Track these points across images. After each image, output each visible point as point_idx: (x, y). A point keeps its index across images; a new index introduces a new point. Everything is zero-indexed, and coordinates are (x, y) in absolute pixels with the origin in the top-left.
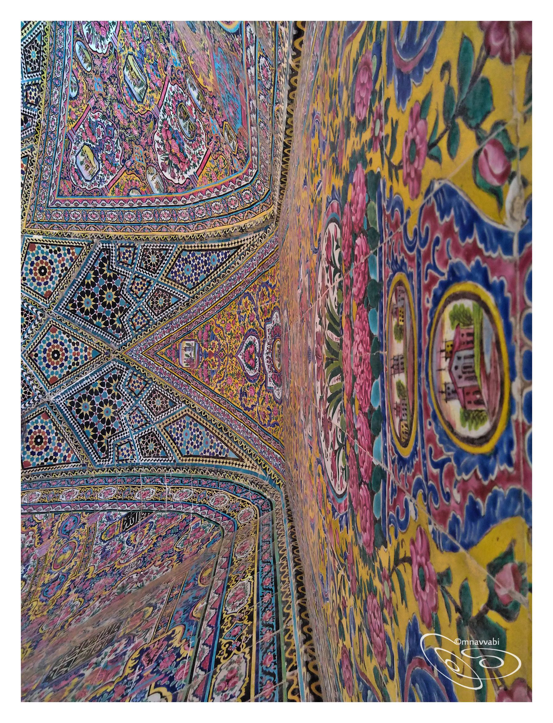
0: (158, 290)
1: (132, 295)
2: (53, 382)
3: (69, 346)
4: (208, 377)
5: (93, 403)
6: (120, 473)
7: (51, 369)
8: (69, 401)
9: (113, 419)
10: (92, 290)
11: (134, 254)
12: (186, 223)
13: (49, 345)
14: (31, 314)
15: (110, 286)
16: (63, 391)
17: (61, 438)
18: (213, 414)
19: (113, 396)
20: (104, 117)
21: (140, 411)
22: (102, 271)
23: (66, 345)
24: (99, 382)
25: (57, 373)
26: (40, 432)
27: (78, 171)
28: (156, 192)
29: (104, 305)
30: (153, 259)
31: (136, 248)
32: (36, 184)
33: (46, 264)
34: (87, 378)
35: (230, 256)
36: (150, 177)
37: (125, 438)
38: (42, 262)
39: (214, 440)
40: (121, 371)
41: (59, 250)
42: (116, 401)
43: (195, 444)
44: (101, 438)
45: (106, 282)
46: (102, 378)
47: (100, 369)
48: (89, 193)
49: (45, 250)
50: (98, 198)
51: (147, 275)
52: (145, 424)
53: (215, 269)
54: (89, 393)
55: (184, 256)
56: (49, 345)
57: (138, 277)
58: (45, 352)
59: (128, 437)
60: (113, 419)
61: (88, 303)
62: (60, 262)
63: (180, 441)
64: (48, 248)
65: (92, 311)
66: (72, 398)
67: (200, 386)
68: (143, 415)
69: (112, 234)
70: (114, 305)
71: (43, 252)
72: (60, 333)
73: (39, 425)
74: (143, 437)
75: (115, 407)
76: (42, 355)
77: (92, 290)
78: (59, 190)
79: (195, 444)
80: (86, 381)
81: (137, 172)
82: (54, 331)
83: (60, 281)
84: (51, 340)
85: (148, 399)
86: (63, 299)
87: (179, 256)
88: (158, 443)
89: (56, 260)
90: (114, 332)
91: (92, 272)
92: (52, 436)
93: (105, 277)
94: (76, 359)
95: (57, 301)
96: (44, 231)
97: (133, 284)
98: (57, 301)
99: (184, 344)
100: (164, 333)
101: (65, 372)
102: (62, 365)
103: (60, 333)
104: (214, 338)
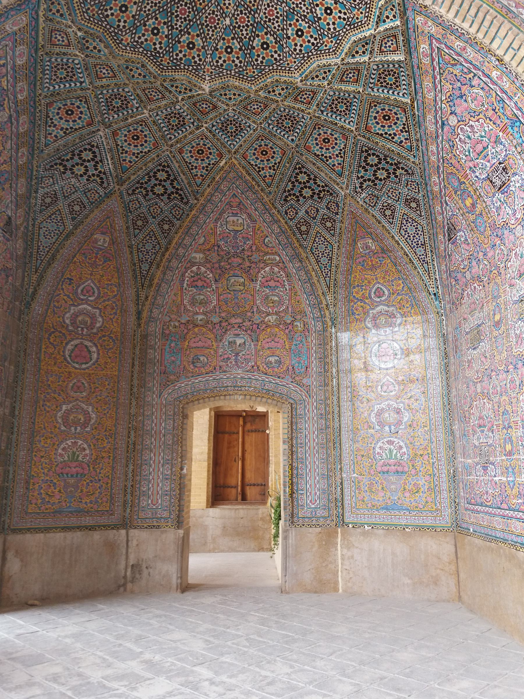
0: (147, 222)
1: (153, 203)
2: (115, 134)
3: (138, 149)
4: (84, 254)
5: (89, 161)
6: (33, 183)
7: (126, 133)
8: (95, 144)
9: (73, 173)
10: (169, 182)
11: (175, 217)
12: (170, 261)
13: (146, 136)
14: (175, 130)
15: (165, 193)
16: (105, 143)
17: (67, 132)
18: (63, 254)
19: (89, 176)
20: (243, 250)
21: (73, 193)
22: (177, 193)
23: (140, 147)
24: (103, 170)
25: (121, 137)
26: (77, 114)
27: (235, 215)
28: (194, 255)
29: (155, 185)
30: (166, 227)
31: (178, 220)
32: (250, 185)
33: (204, 157)
34: (108, 164)
35: (142, 278)
36: (202, 256)
37: (57, 181)
38: (206, 154)
39: (47, 249)
40: (105, 188)
41: (207, 170)
42: (85, 177)
43: (47, 233)
44: (61, 164)
45: (169, 192)
46: (104, 173)
47: (111, 175)
48: (221, 214)
49: (213, 162)
50: (215, 217)
51: (160, 218)
52: (64, 196)
53: (140, 266)
54: (97, 162)
55: (158, 247)
56: (146, 136)
57: (161, 212)
58: (141, 131)
59: (58, 183)
60: (73, 173)
61: (162, 176)
62: (200, 166)
63: (49, 221)
64: (213, 164)
65: (154, 176)
66: (97, 147)
67: (80, 246)
68: (71, 195)
69: (193, 212)
70: (152, 191)
71: (212, 159)
72: (150, 148)
73: (83, 116)
74: (55, 194)
75: (81, 176)
76: (140, 128)
77: (169, 182)
78: (236, 196)
79: (47, 233)
80: (106, 162)
81: (209, 250)
82: (154, 144)
83: (186, 162)
84: (148, 139)
85: (81, 201)
86: (172, 162)
87: (159, 244)
88: (50, 205)
89: (202, 164)
90: (134, 188)
91: (179, 188)
92: (71, 124)
93: (172, 193)
94: (126, 152)
95: (173, 159)
96: (222, 172)
97: (159, 207)
98: (173, 159)
99: (107, 239)
100: (119, 227)
101: (119, 143)
102: (126, 141)
103: (150, 148)
104: (105, 262)
